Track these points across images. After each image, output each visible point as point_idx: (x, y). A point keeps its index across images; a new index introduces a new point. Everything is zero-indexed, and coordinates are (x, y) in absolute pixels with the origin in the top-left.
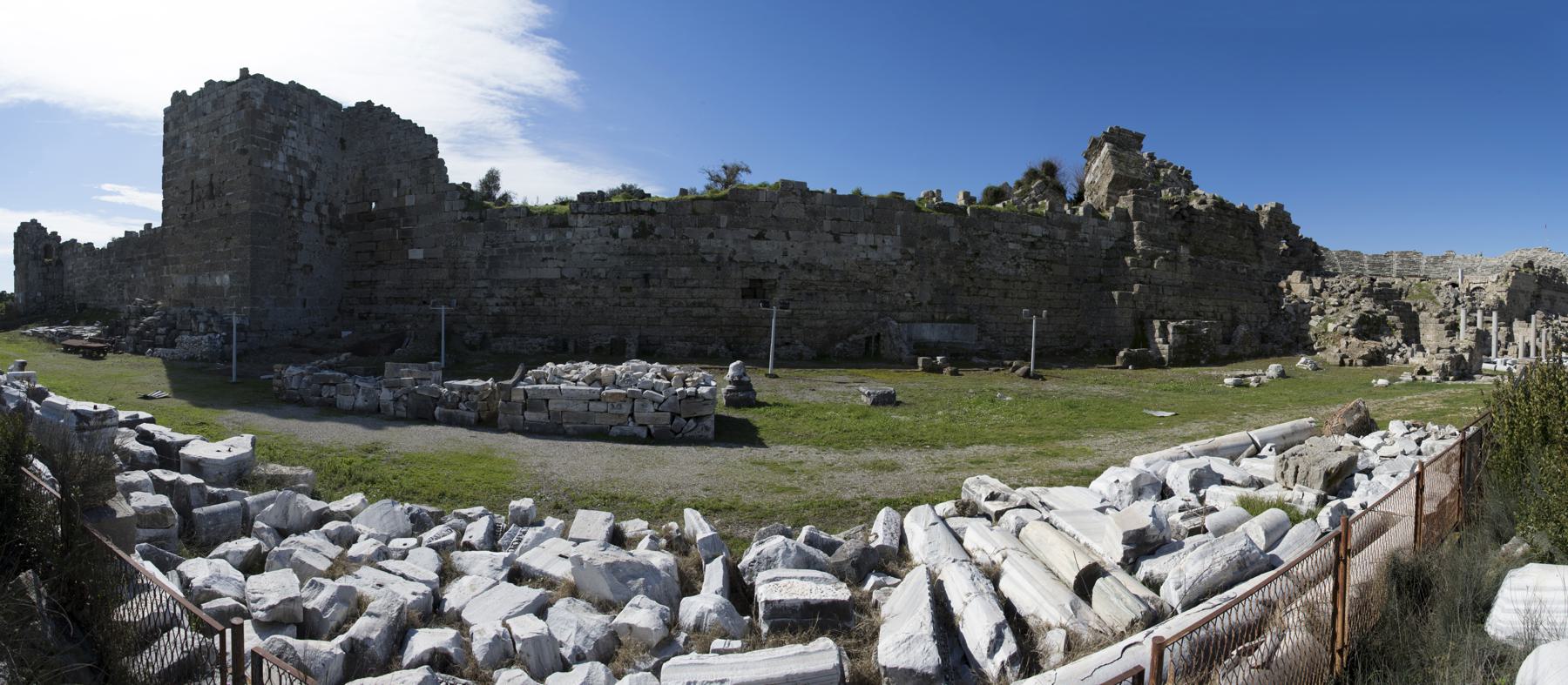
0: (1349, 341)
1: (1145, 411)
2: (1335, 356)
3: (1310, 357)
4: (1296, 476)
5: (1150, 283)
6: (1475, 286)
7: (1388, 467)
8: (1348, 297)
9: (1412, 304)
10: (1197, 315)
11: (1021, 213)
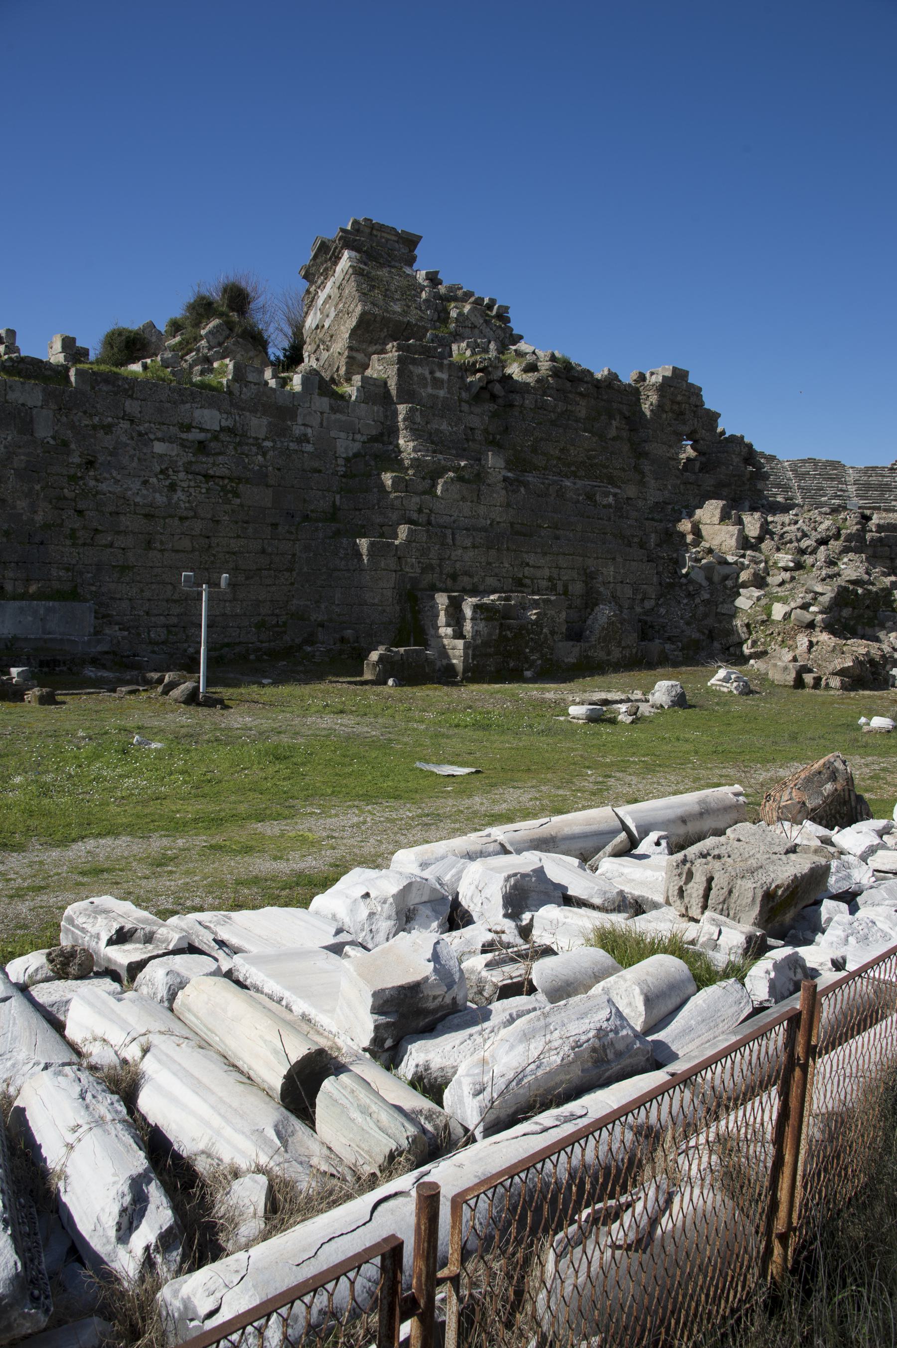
0: (814, 640)
1: (418, 764)
2: (786, 668)
3: (735, 669)
5: (429, 523)
7: (890, 891)
8: (814, 552)
10: (519, 584)
11: (179, 383)
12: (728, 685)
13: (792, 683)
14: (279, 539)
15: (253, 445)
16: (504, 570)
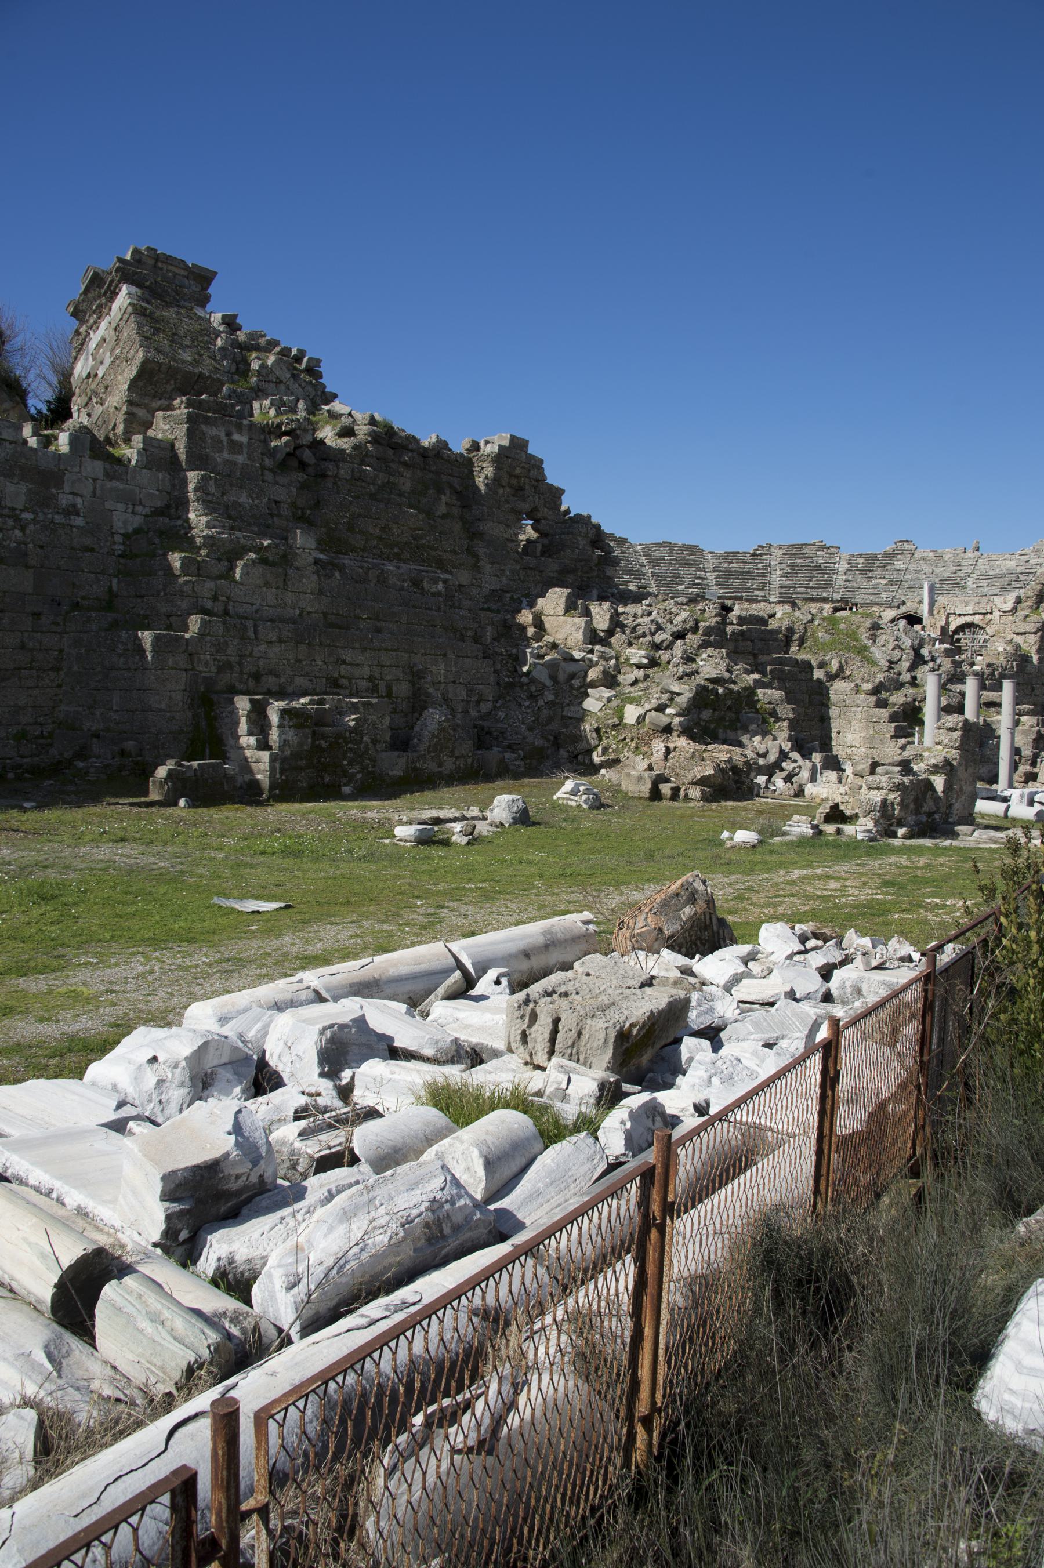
0: (671, 746)
1: (216, 900)
2: (640, 778)
3: (584, 780)
4: (553, 1040)
5: (226, 613)
6: (962, 621)
7: (756, 1025)
8: (670, 647)
9: (814, 664)
10: (335, 685)
12: (576, 798)
13: (648, 795)
14: (42, 632)
15: (9, 517)
16: (317, 668)
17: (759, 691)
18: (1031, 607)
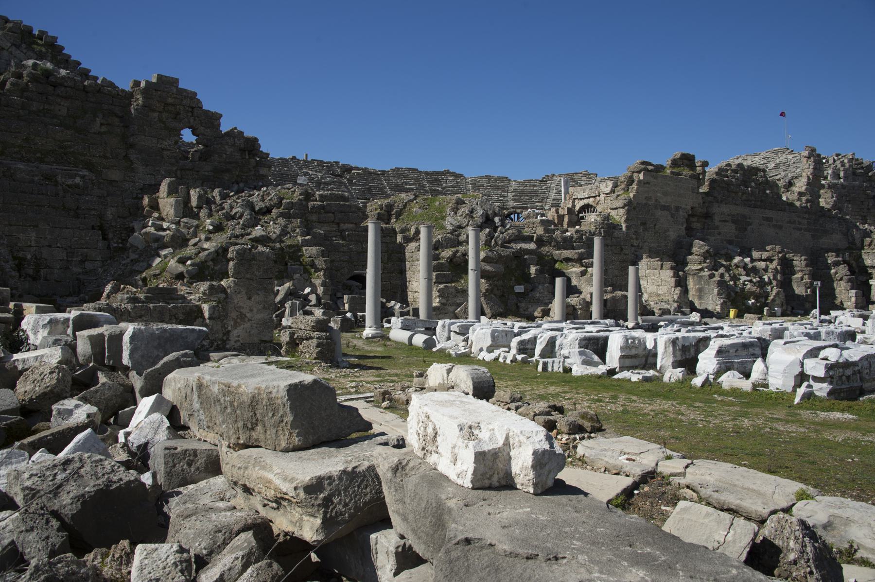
17: (304, 248)
18: (623, 189)
